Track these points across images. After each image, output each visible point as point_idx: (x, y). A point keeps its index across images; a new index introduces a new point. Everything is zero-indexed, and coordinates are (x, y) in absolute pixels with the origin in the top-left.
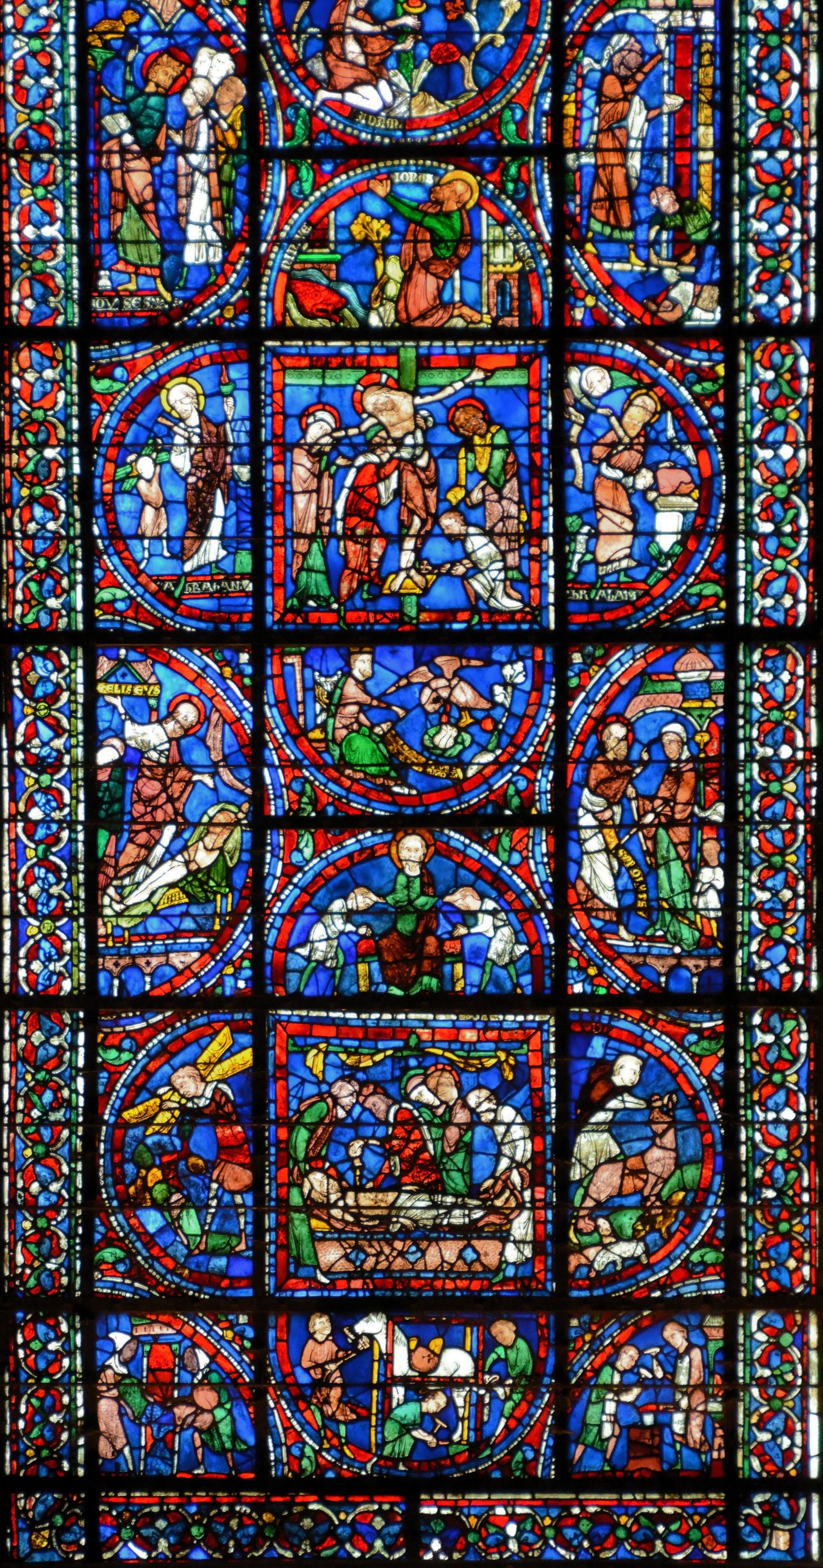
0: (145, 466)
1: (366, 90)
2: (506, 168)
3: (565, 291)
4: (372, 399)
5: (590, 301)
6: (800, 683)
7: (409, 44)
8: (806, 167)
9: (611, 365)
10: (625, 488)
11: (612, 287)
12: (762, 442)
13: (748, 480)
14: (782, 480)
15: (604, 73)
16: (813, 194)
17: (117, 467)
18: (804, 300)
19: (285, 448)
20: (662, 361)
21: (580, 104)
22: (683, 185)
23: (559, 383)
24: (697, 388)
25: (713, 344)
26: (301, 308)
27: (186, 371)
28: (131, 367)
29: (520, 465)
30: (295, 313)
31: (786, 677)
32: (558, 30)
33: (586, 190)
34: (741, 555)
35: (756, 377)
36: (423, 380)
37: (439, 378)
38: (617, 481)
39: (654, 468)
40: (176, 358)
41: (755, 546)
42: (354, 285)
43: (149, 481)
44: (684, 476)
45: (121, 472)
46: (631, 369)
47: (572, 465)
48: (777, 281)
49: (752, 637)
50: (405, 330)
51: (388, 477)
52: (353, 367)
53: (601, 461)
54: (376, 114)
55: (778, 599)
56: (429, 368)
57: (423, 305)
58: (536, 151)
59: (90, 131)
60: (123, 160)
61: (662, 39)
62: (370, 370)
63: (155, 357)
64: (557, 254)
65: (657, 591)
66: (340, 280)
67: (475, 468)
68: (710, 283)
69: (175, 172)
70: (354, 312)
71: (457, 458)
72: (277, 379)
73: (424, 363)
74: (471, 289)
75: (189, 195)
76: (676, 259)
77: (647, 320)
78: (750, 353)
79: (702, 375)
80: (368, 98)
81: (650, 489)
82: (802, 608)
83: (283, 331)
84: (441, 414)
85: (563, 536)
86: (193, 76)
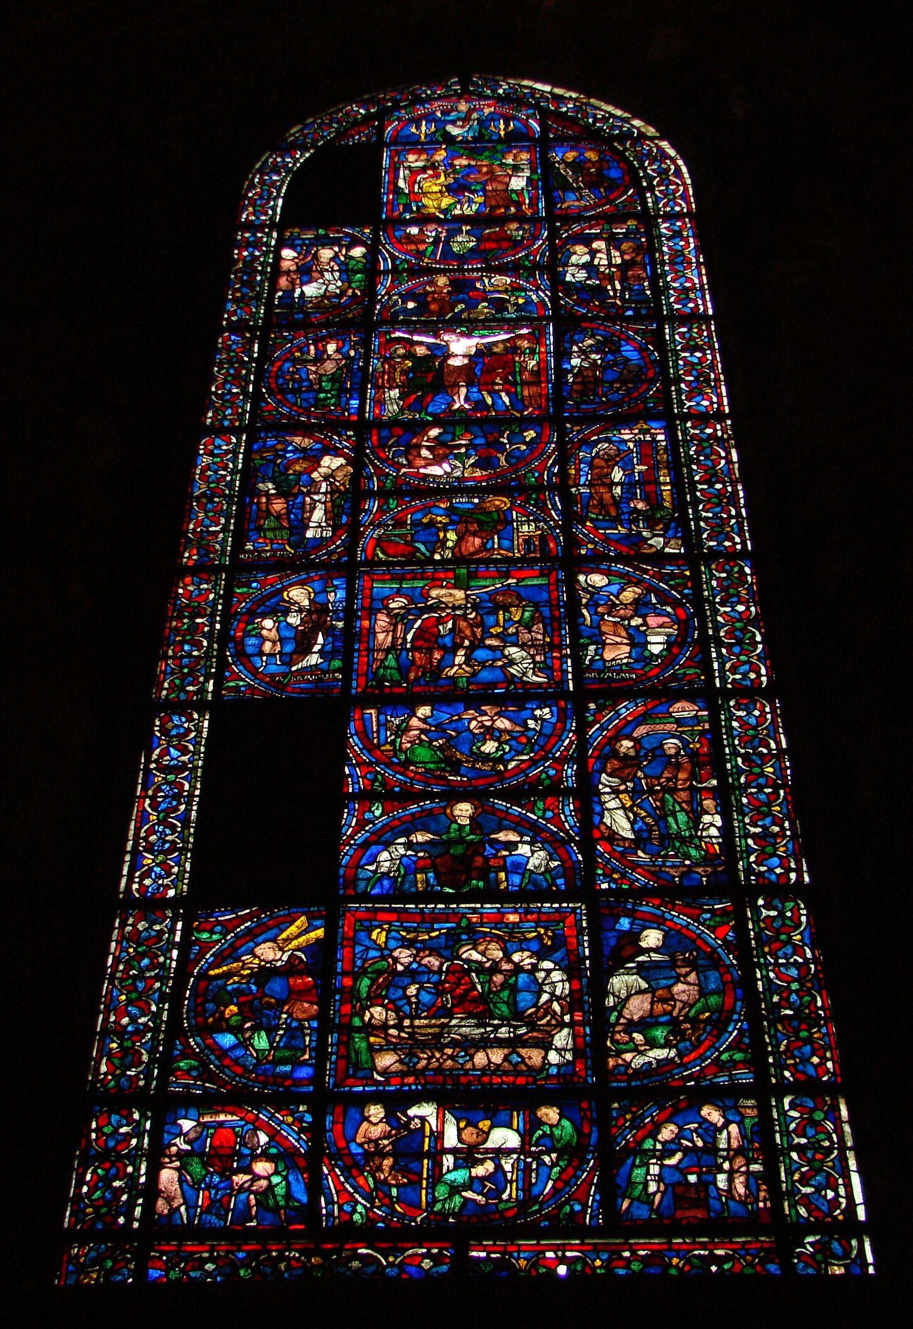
0: (268, 623)
1: (437, 468)
2: (530, 495)
3: (573, 542)
4: (434, 593)
5: (590, 546)
6: (769, 716)
7: (463, 450)
8: (735, 491)
9: (607, 573)
10: (623, 625)
11: (606, 539)
12: (722, 604)
13: (715, 621)
14: (739, 621)
15: (593, 458)
16: (742, 501)
17: (248, 624)
18: (743, 543)
19: (371, 613)
20: (646, 571)
21: (578, 470)
22: (653, 499)
23: (571, 582)
24: (672, 583)
25: (680, 562)
26: (383, 553)
27: (302, 583)
28: (263, 584)
29: (544, 617)
30: (381, 555)
31: (757, 713)
32: (561, 445)
33: (585, 502)
34: (714, 655)
35: (714, 578)
36: (473, 584)
37: (483, 583)
38: (615, 623)
39: (644, 617)
40: (294, 578)
41: (724, 651)
42: (423, 543)
43: (270, 630)
44: (667, 620)
45: (250, 627)
46: (621, 575)
47: (583, 616)
48: (723, 536)
49: (727, 694)
50: (459, 559)
51: (446, 622)
52: (422, 579)
53: (604, 614)
54: (441, 476)
55: (745, 675)
56: (477, 578)
57: (472, 549)
58: (551, 487)
59: (249, 489)
60: (268, 499)
61: (631, 445)
62: (433, 579)
63: (280, 578)
64: (566, 529)
65: (652, 674)
66: (413, 540)
67: (510, 619)
68: (675, 537)
69: (304, 502)
70: (423, 554)
71: (497, 614)
72: (367, 585)
73: (472, 576)
74: (506, 543)
75: (312, 511)
76: (651, 528)
77: (632, 553)
78: (708, 566)
79: (672, 576)
80: (436, 470)
81: (642, 625)
82: (764, 679)
83: (372, 563)
84: (486, 597)
85: (578, 651)
86: (320, 466)
